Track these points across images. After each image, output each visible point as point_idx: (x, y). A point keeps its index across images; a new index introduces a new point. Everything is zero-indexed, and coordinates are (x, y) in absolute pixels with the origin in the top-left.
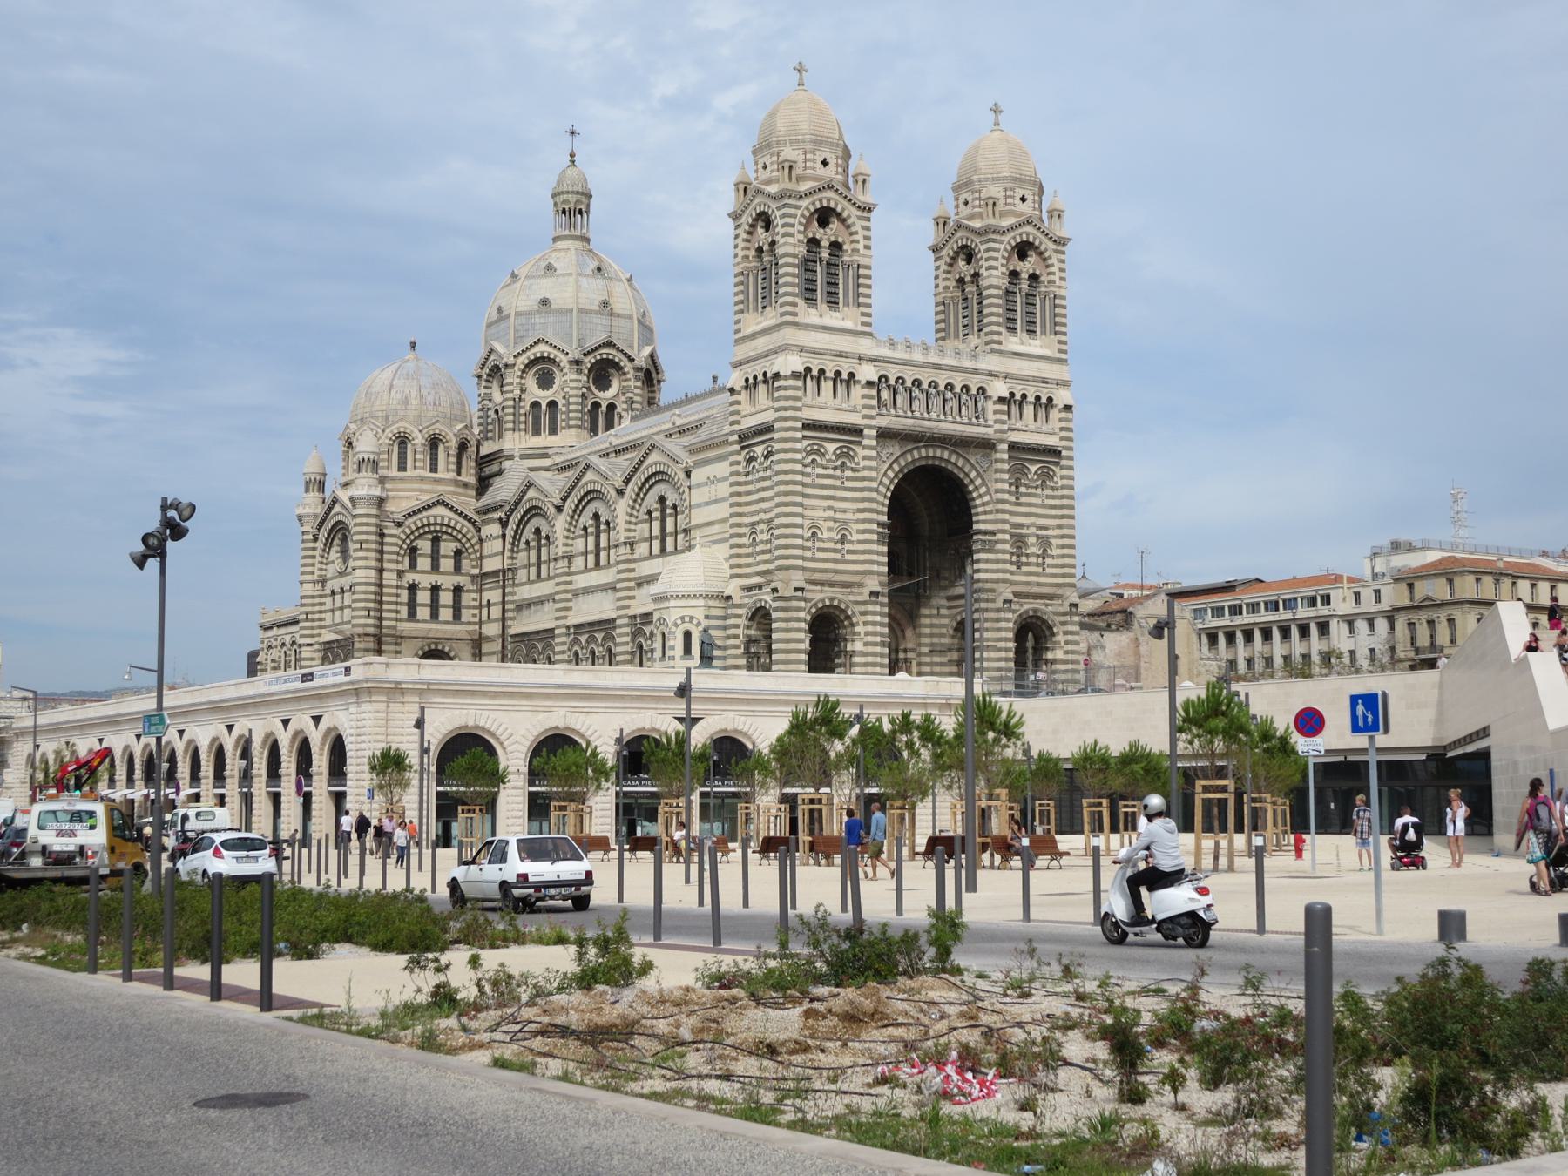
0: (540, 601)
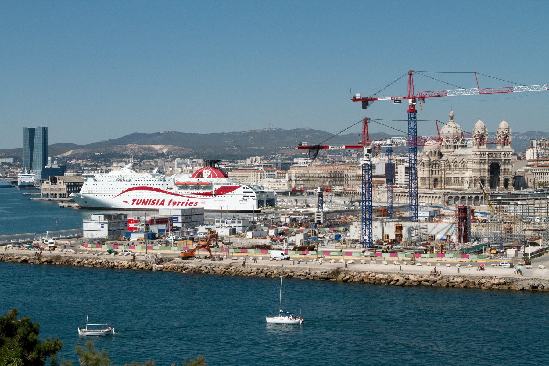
0: (450, 173)
